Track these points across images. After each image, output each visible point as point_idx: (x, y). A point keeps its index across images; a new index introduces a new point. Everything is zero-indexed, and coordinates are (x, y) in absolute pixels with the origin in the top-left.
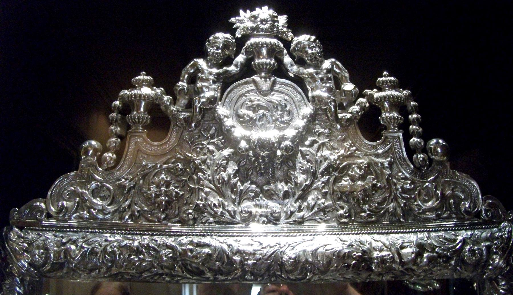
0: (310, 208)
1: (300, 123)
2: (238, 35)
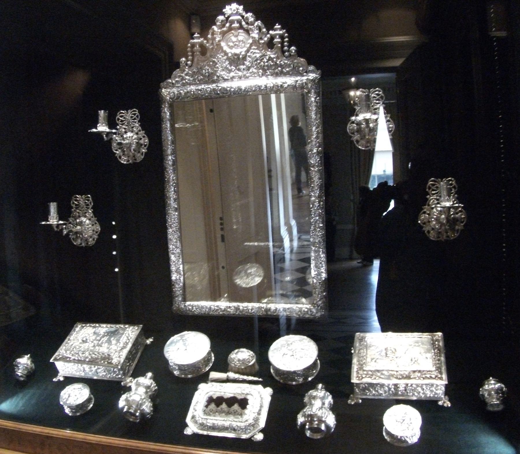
0: (250, 73)
1: (248, 46)
2: (226, 16)
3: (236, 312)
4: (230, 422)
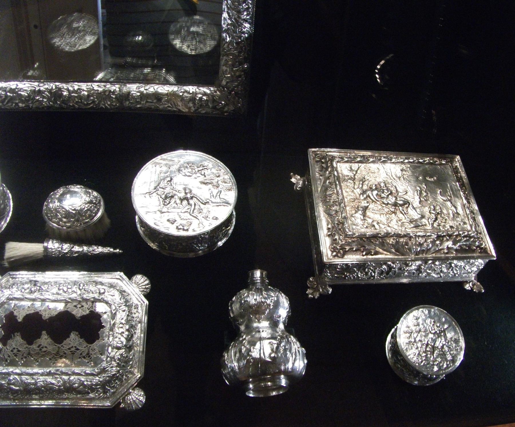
3: (55, 102)
4: (66, 378)
